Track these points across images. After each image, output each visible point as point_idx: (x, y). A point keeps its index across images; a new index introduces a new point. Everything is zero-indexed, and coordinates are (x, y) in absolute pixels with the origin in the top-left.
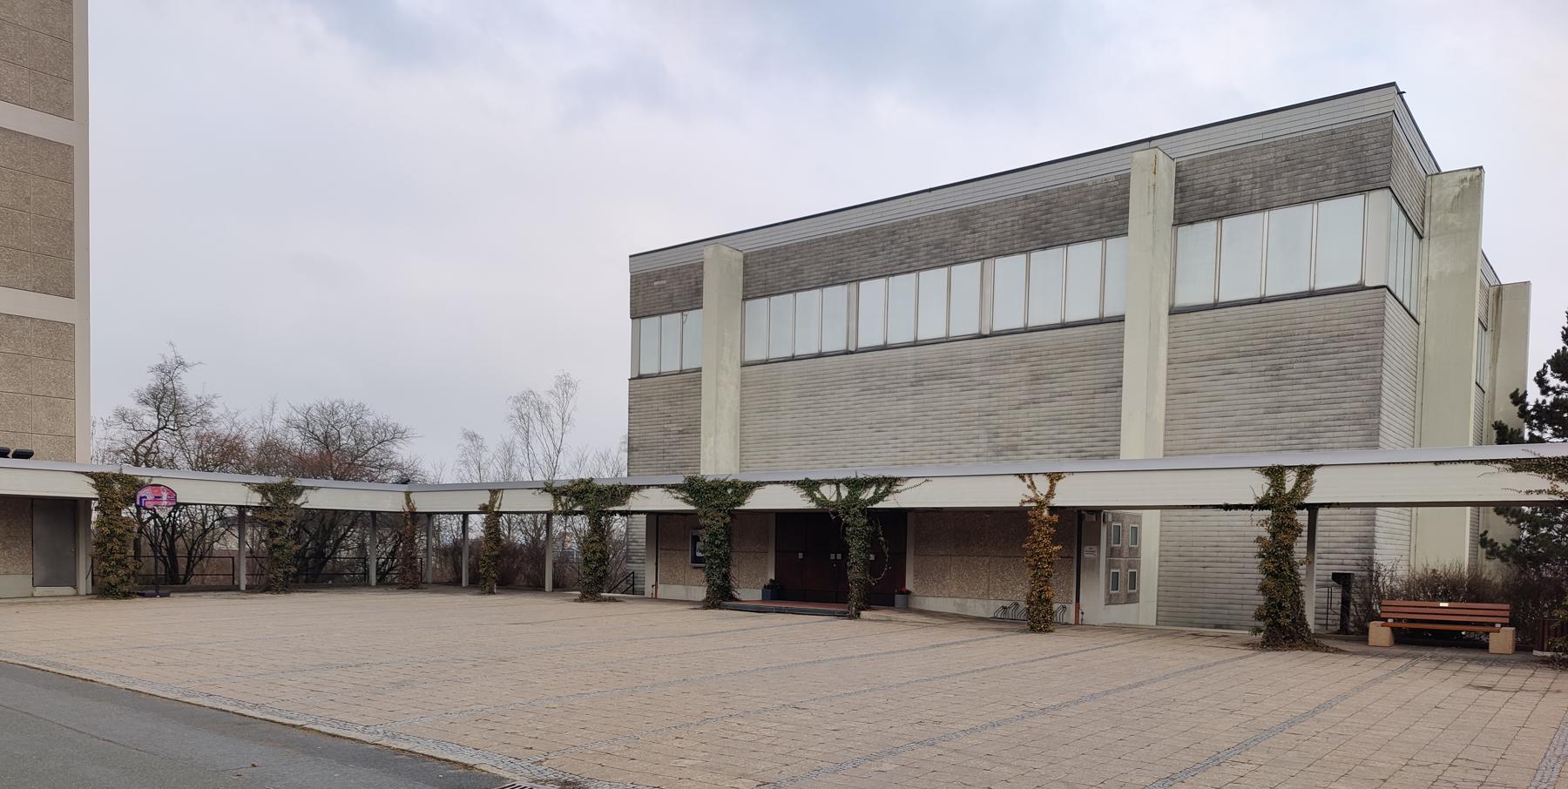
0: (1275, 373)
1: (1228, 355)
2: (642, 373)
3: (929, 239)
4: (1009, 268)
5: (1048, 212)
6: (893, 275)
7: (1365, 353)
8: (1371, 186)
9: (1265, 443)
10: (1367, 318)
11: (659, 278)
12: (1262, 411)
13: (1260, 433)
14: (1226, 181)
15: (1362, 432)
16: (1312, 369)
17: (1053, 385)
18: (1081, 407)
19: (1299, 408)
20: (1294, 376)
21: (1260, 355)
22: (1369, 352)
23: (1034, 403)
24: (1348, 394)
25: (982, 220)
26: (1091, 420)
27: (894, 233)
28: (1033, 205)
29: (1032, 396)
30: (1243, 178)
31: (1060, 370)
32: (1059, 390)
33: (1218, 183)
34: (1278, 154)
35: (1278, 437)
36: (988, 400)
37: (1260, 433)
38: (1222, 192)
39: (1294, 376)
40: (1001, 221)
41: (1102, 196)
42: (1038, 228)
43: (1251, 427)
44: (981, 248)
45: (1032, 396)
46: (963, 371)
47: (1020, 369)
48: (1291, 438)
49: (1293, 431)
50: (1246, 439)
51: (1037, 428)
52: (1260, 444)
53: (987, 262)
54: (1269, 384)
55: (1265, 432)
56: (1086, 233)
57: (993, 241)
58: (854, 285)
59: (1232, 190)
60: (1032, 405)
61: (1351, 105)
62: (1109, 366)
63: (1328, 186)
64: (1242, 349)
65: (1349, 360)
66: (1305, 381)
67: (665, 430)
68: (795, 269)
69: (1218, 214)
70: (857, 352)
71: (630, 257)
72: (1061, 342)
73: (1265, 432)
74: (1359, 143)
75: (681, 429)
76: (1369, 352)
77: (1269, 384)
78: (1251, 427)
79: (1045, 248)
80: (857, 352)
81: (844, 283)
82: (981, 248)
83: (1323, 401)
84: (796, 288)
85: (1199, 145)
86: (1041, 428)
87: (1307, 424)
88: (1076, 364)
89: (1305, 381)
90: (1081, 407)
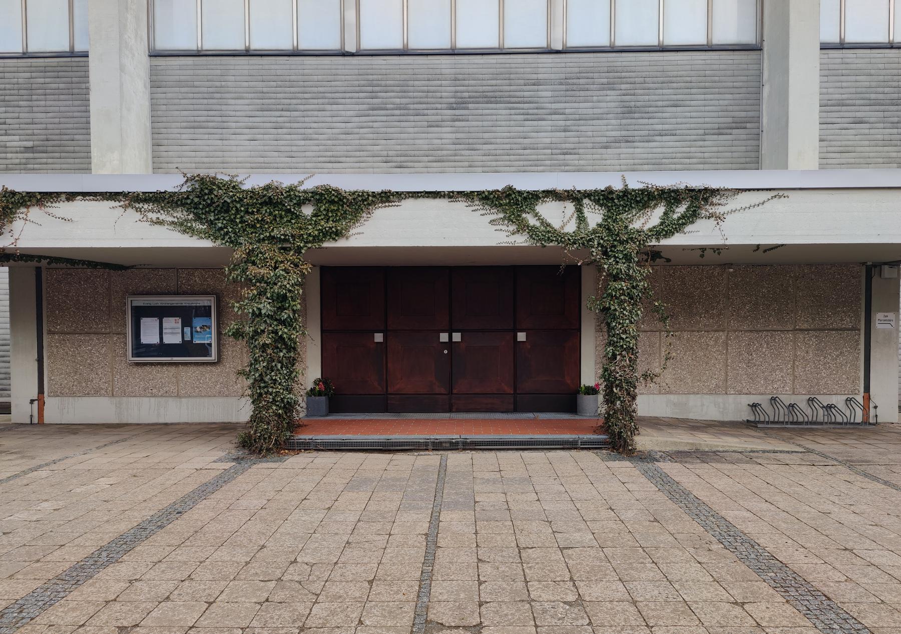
1: (858, 102)
17: (651, 121)
18: (688, 149)
21: (893, 105)
23: (627, 141)
31: (660, 103)
32: (660, 127)
45: (624, 133)
46: (526, 94)
47: (608, 98)
60: (623, 145)
64: (873, 96)
72: (661, 68)
75: (30, 144)
88: (679, 97)
90: (688, 149)
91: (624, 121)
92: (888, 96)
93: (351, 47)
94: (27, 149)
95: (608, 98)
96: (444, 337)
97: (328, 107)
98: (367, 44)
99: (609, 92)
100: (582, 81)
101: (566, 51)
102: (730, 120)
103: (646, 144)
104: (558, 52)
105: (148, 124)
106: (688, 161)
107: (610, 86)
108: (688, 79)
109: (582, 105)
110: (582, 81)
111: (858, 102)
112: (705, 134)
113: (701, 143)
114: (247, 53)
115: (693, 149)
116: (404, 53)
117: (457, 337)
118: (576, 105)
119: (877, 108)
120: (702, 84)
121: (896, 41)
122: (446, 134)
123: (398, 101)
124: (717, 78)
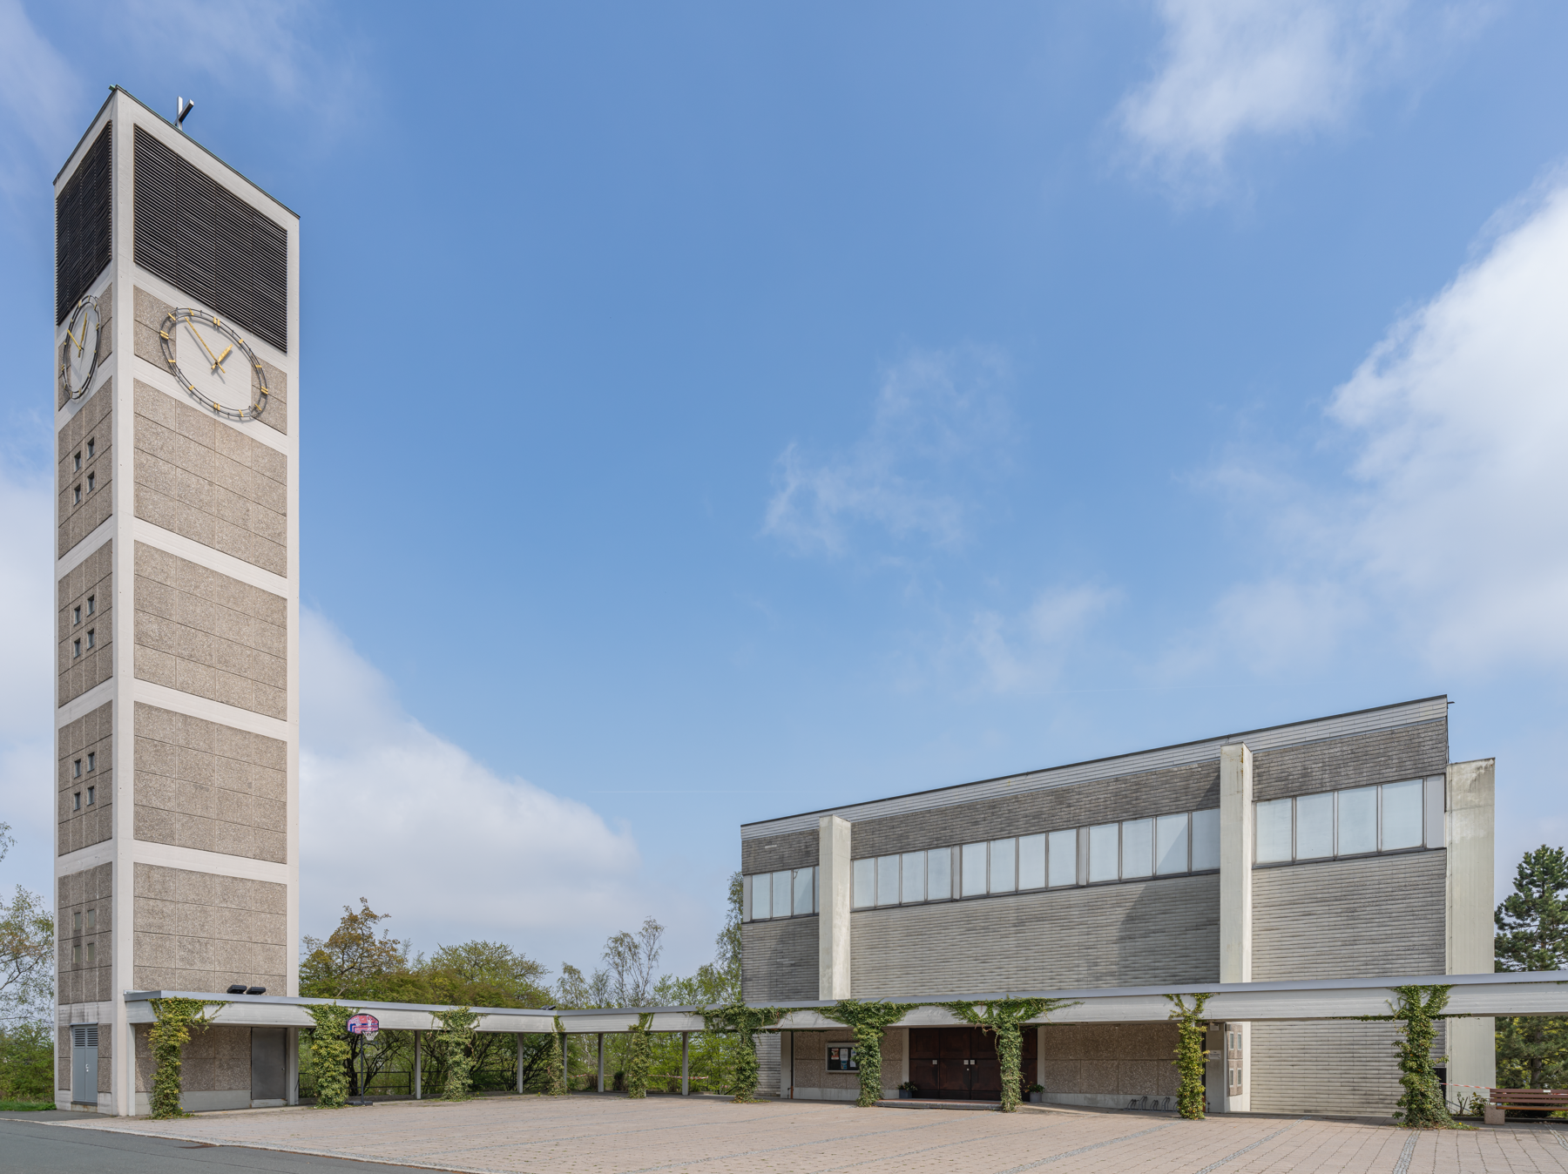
0: (1350, 914)
1: (1306, 901)
2: (754, 918)
3: (1028, 812)
4: (1102, 837)
5: (1137, 791)
6: (994, 840)
7: (1430, 899)
8: (1429, 773)
9: (1343, 968)
10: (1430, 873)
11: (770, 843)
12: (1340, 943)
13: (1339, 960)
14: (1299, 768)
15: (1431, 959)
16: (1384, 911)
19: (1373, 941)
20: (1368, 917)
21: (1336, 900)
22: (1434, 899)
24: (1416, 930)
25: (1077, 797)
26: (1184, 951)
27: (994, 807)
28: (1123, 786)
29: (1128, 933)
30: (1313, 766)
31: (1154, 913)
32: (1153, 928)
33: (1292, 769)
34: (1344, 748)
35: (1355, 964)
36: (1086, 937)
37: (1339, 960)
38: (1295, 777)
39: (1368, 917)
40: (1094, 798)
41: (1187, 779)
42: (1128, 803)
43: (1331, 956)
44: (1076, 818)
45: (1128, 933)
46: (1062, 914)
47: (1117, 912)
48: (1367, 965)
49: (1368, 959)
50: (1327, 965)
51: (1134, 958)
52: (1339, 969)
53: (1083, 831)
54: (1345, 922)
55: (1343, 960)
56: (1174, 807)
57: (1087, 813)
58: (957, 849)
59: (1304, 775)
60: (1127, 940)
61: (1408, 712)
62: (1198, 909)
63: (1390, 773)
65: (1416, 904)
66: (1377, 920)
67: (777, 963)
68: (901, 835)
69: (1292, 794)
70: (961, 900)
71: (742, 826)
72: (1154, 891)
73: (1343, 960)
74: (1417, 740)
75: (793, 962)
76: (1434, 899)
77: (1345, 922)
78: (1331, 956)
79: (1136, 819)
80: (961, 900)
81: (948, 846)
82: (1076, 818)
83: (1394, 936)
84: (901, 851)
85: (1272, 741)
86: (1137, 958)
87: (1381, 954)
89: (1377, 920)
91: (1128, 926)
92: (1333, 895)
93: (957, 896)
94: (792, 965)
95: (1117, 912)
96: (966, 1062)
97: (943, 931)
98: (966, 893)
99: (1117, 909)
100: (1099, 903)
101: (1089, 885)
102: (1205, 920)
103: (1144, 939)
104: (1083, 887)
105: (849, 949)
106: (1174, 948)
107: (1118, 905)
108: (1174, 896)
109: (1099, 918)
110: (1099, 903)
111: (1306, 901)
112: (1187, 930)
113: (1184, 936)
114: (900, 906)
115: (1177, 941)
116: (988, 896)
117: (973, 1062)
118: (1095, 918)
119: (1323, 904)
120: (1184, 898)
121: (1339, 854)
122: (1012, 941)
123: (983, 924)
124: (1195, 894)
